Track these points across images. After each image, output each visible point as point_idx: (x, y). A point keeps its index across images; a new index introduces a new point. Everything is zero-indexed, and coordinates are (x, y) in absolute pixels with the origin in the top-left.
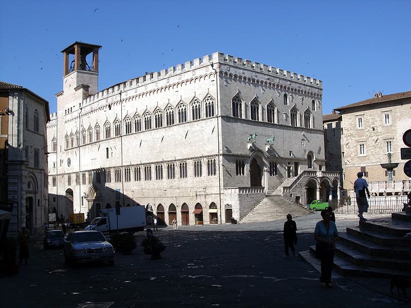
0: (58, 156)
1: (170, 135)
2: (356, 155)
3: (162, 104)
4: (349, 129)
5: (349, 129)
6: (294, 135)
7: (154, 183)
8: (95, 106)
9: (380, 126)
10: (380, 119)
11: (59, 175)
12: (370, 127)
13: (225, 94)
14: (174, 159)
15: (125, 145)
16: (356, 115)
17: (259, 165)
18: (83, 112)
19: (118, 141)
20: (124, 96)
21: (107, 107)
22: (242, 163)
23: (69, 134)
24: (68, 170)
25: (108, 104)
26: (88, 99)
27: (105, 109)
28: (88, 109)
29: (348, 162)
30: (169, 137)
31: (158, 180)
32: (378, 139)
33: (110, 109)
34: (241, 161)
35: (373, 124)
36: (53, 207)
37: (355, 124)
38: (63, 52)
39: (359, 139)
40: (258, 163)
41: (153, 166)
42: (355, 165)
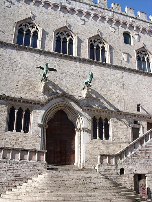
6: (145, 83)
13: (4, 16)
34: (24, 109)
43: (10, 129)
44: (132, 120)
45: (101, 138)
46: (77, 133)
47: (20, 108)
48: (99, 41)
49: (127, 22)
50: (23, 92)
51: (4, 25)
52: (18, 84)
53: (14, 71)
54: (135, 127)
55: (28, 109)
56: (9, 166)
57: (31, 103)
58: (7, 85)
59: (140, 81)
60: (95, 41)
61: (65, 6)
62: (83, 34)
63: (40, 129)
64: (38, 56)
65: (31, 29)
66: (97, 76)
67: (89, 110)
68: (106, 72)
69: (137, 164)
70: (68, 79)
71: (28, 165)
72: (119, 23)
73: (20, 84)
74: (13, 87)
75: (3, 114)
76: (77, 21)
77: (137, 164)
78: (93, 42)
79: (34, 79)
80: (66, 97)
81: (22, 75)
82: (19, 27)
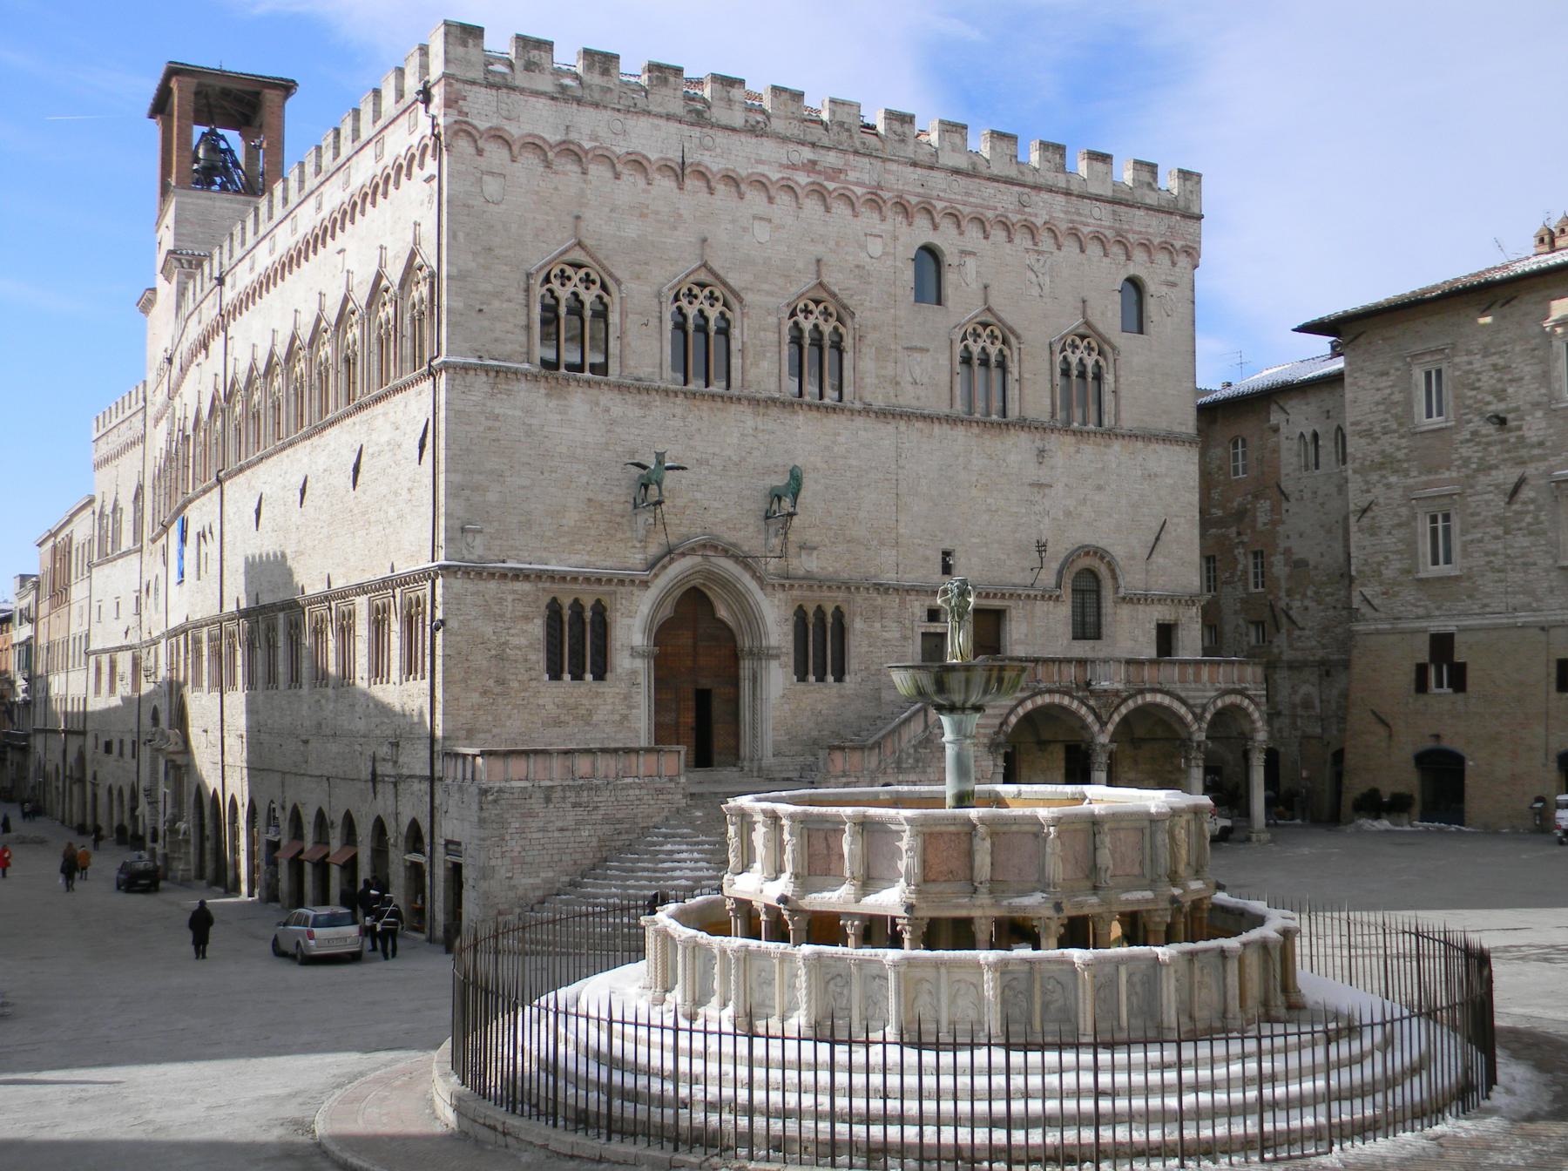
2: (1408, 572)
4: (1377, 429)
5: (1377, 429)
9: (1537, 405)
10: (1538, 370)
11: (155, 642)
12: (1481, 414)
16: (1418, 348)
17: (731, 623)
22: (588, 615)
29: (1365, 609)
32: (1521, 482)
33: (207, 357)
34: (588, 602)
35: (1500, 395)
37: (1409, 404)
38: (151, 116)
39: (1427, 485)
40: (722, 613)
42: (1402, 625)
43: (555, 674)
44: (918, 608)
45: (821, 678)
46: (742, 662)
47: (576, 601)
48: (821, 307)
49: (934, 202)
50: (581, 547)
51: (490, 288)
52: (564, 522)
53: (546, 474)
54: (932, 630)
55: (598, 601)
56: (596, 799)
57: (610, 581)
58: (530, 528)
59: (961, 459)
60: (807, 311)
61: (699, 164)
62: (765, 287)
63: (640, 665)
64: (617, 405)
65: (581, 289)
66: (812, 459)
67: (783, 586)
68: (841, 439)
69: (929, 770)
70: (720, 483)
71: (644, 792)
72: (899, 209)
73: (571, 519)
74: (550, 534)
75: (529, 627)
76: (745, 229)
77: (929, 770)
78: (800, 317)
79: (611, 498)
80: (715, 548)
81: (574, 485)
82: (542, 286)
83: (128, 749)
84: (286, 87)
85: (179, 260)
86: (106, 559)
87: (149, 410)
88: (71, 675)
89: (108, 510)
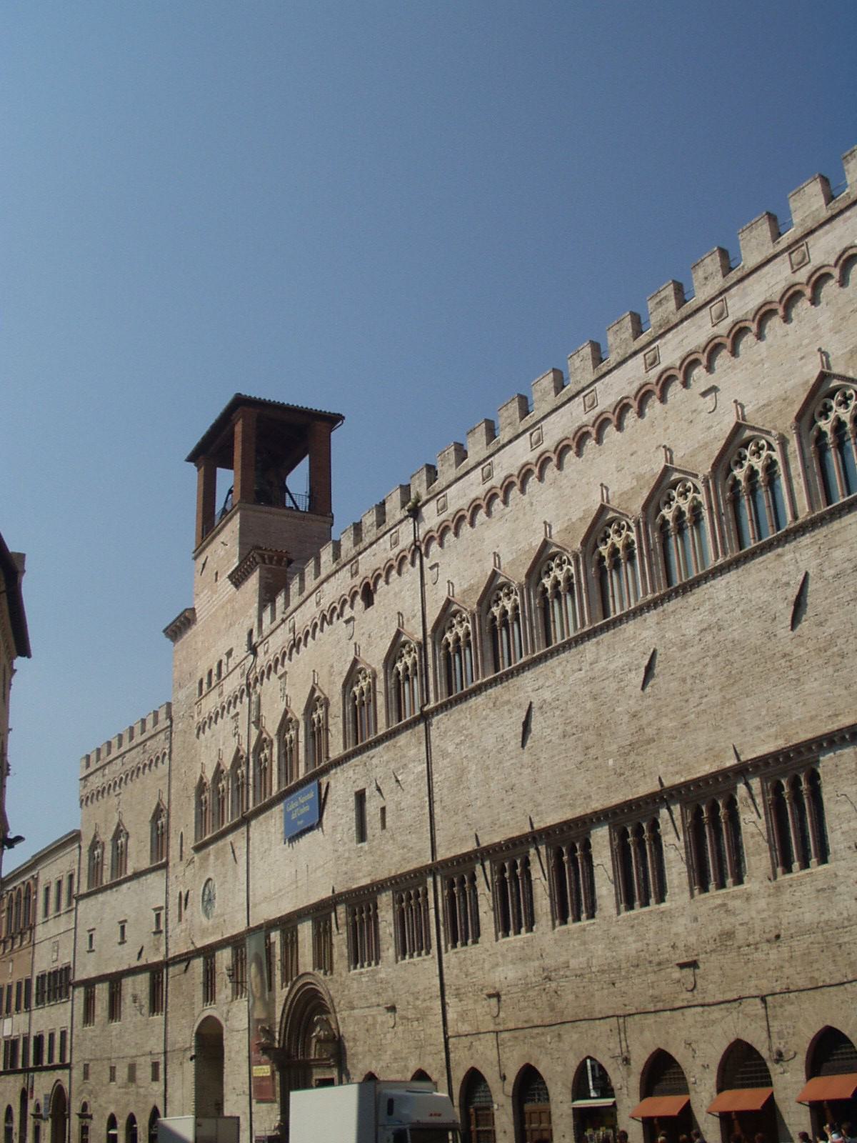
0: (172, 878)
1: (691, 632)
3: (628, 484)
7: (614, 930)
8: (306, 615)
14: (731, 762)
15: (445, 755)
18: (263, 660)
19: (409, 743)
20: (431, 518)
21: (358, 598)
23: (209, 776)
24: (204, 932)
25: (358, 580)
26: (280, 600)
27: (348, 612)
28: (280, 640)
30: (684, 646)
31: (638, 910)
36: (151, 1107)
38: (191, 459)
41: (601, 838)
83: (144, 1073)
84: (334, 420)
85: (262, 557)
86: (97, 889)
87: (179, 726)
88: (35, 1014)
89: (107, 837)
